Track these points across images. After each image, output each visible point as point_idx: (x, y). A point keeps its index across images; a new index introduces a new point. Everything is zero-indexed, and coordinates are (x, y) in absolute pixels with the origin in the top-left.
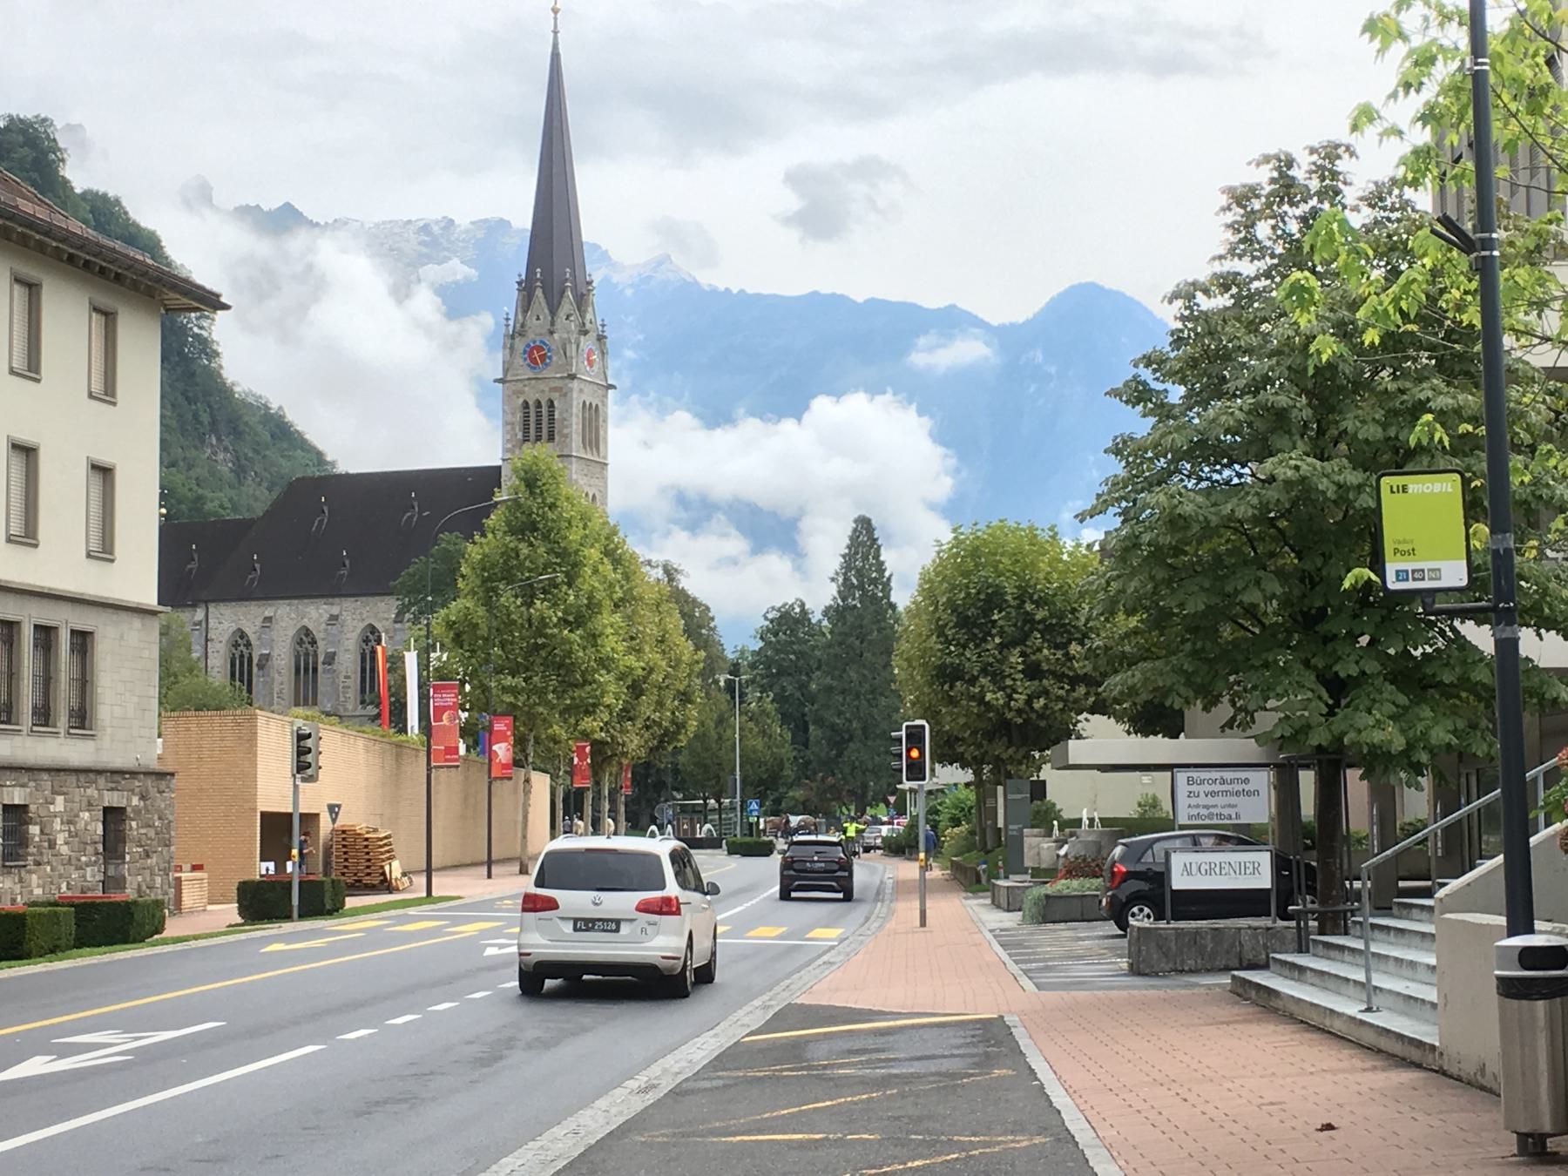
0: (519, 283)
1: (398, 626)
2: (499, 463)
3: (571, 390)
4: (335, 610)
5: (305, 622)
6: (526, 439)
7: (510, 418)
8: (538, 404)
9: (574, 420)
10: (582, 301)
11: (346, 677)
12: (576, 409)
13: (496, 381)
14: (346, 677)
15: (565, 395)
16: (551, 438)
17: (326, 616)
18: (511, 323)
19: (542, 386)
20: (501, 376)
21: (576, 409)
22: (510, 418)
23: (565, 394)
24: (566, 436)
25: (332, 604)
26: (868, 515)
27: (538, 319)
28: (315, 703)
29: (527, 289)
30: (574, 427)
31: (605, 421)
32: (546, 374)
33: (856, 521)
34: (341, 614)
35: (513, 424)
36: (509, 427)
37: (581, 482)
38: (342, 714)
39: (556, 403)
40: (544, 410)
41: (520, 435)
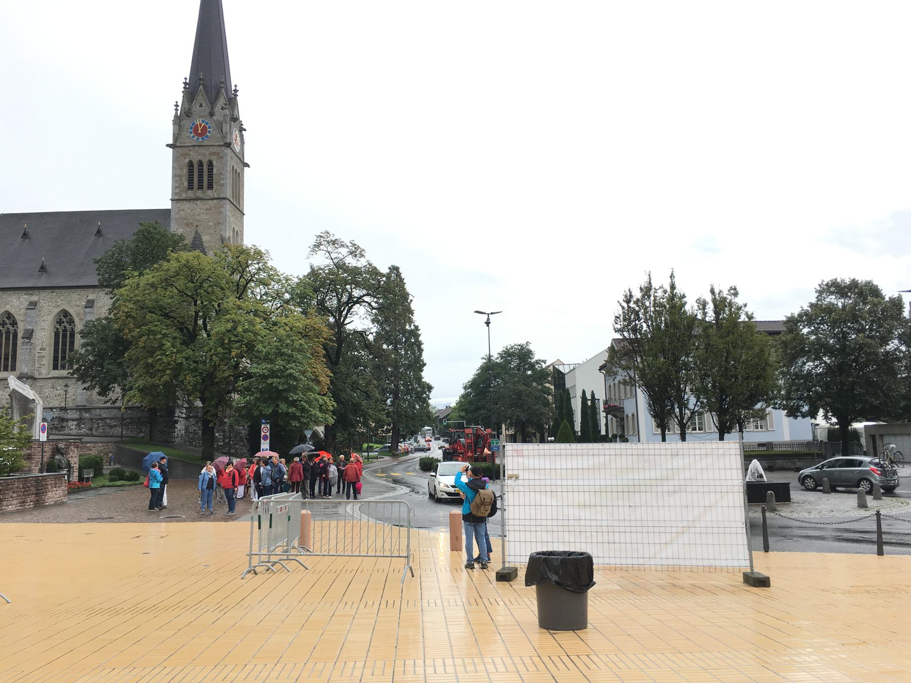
0: (185, 83)
1: (88, 310)
2: (167, 205)
3: (227, 154)
4: (34, 298)
5: (8, 308)
6: (190, 187)
7: (178, 172)
8: (201, 164)
9: (228, 175)
10: (232, 102)
11: (41, 349)
12: (229, 169)
13: (168, 145)
14: (41, 349)
15: (222, 158)
16: (210, 187)
17: (26, 304)
18: (179, 108)
19: (202, 150)
20: (171, 142)
21: (229, 169)
22: (178, 172)
23: (221, 158)
24: (223, 185)
25: (32, 295)
26: (397, 265)
27: (201, 106)
28: (14, 369)
29: (191, 91)
30: (228, 180)
31: (243, 186)
32: (206, 143)
33: (389, 268)
34: (39, 300)
35: (180, 176)
36: (177, 178)
37: (232, 220)
38: (37, 376)
39: (214, 163)
40: (205, 168)
41: (186, 184)
